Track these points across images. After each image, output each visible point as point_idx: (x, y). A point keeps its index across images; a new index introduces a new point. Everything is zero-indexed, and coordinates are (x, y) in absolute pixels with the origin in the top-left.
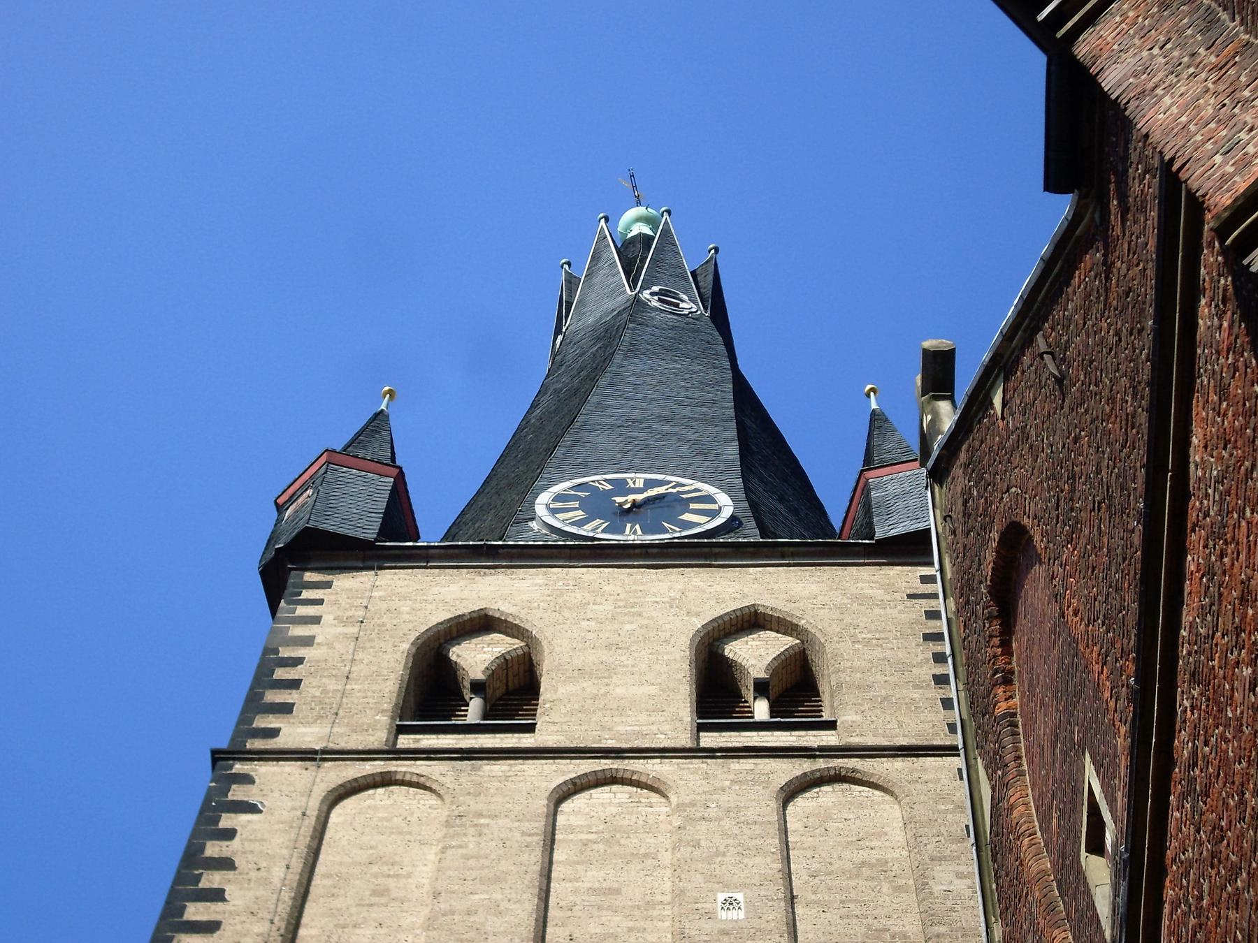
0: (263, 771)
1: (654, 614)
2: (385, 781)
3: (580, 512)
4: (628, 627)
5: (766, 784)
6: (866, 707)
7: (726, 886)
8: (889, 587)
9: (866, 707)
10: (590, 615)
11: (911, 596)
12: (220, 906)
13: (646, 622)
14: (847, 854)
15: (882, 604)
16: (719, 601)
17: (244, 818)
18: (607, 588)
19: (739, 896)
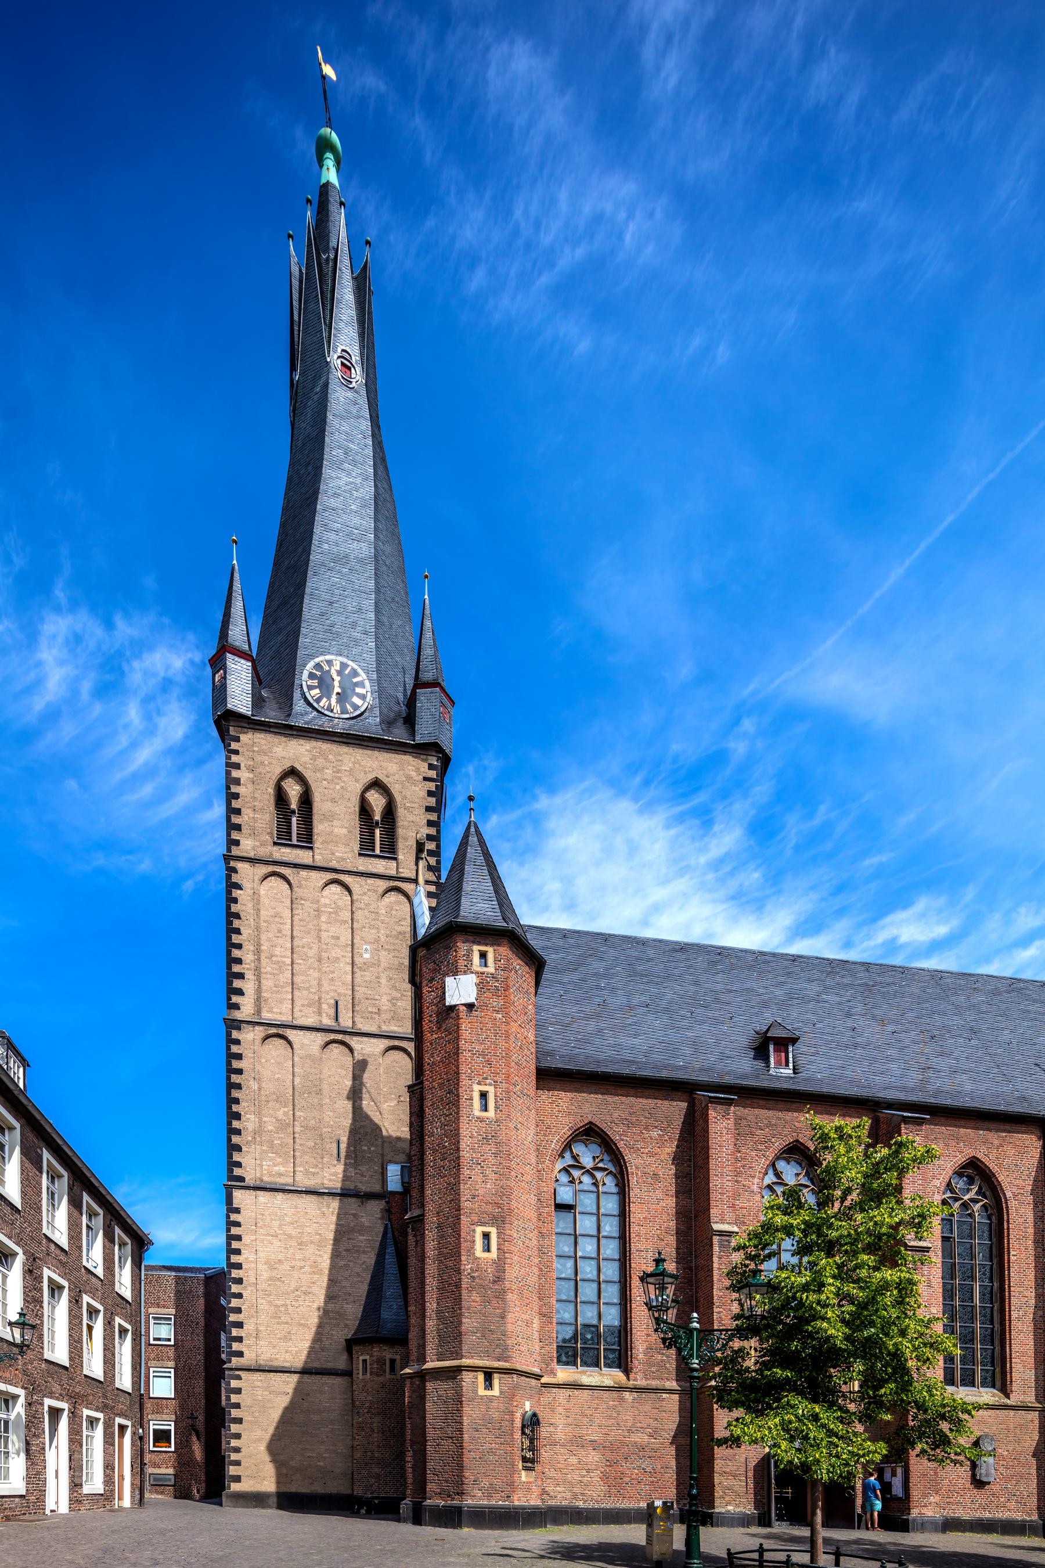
0: (240, 866)
1: (345, 779)
2: (274, 874)
3: (317, 691)
4: (338, 787)
5: (376, 891)
6: (405, 851)
7: (366, 943)
8: (417, 770)
9: (405, 851)
10: (325, 777)
11: (425, 779)
12: (240, 937)
13: (343, 784)
14: (396, 928)
15: (414, 783)
16: (365, 773)
17: (239, 892)
18: (330, 757)
19: (368, 947)
